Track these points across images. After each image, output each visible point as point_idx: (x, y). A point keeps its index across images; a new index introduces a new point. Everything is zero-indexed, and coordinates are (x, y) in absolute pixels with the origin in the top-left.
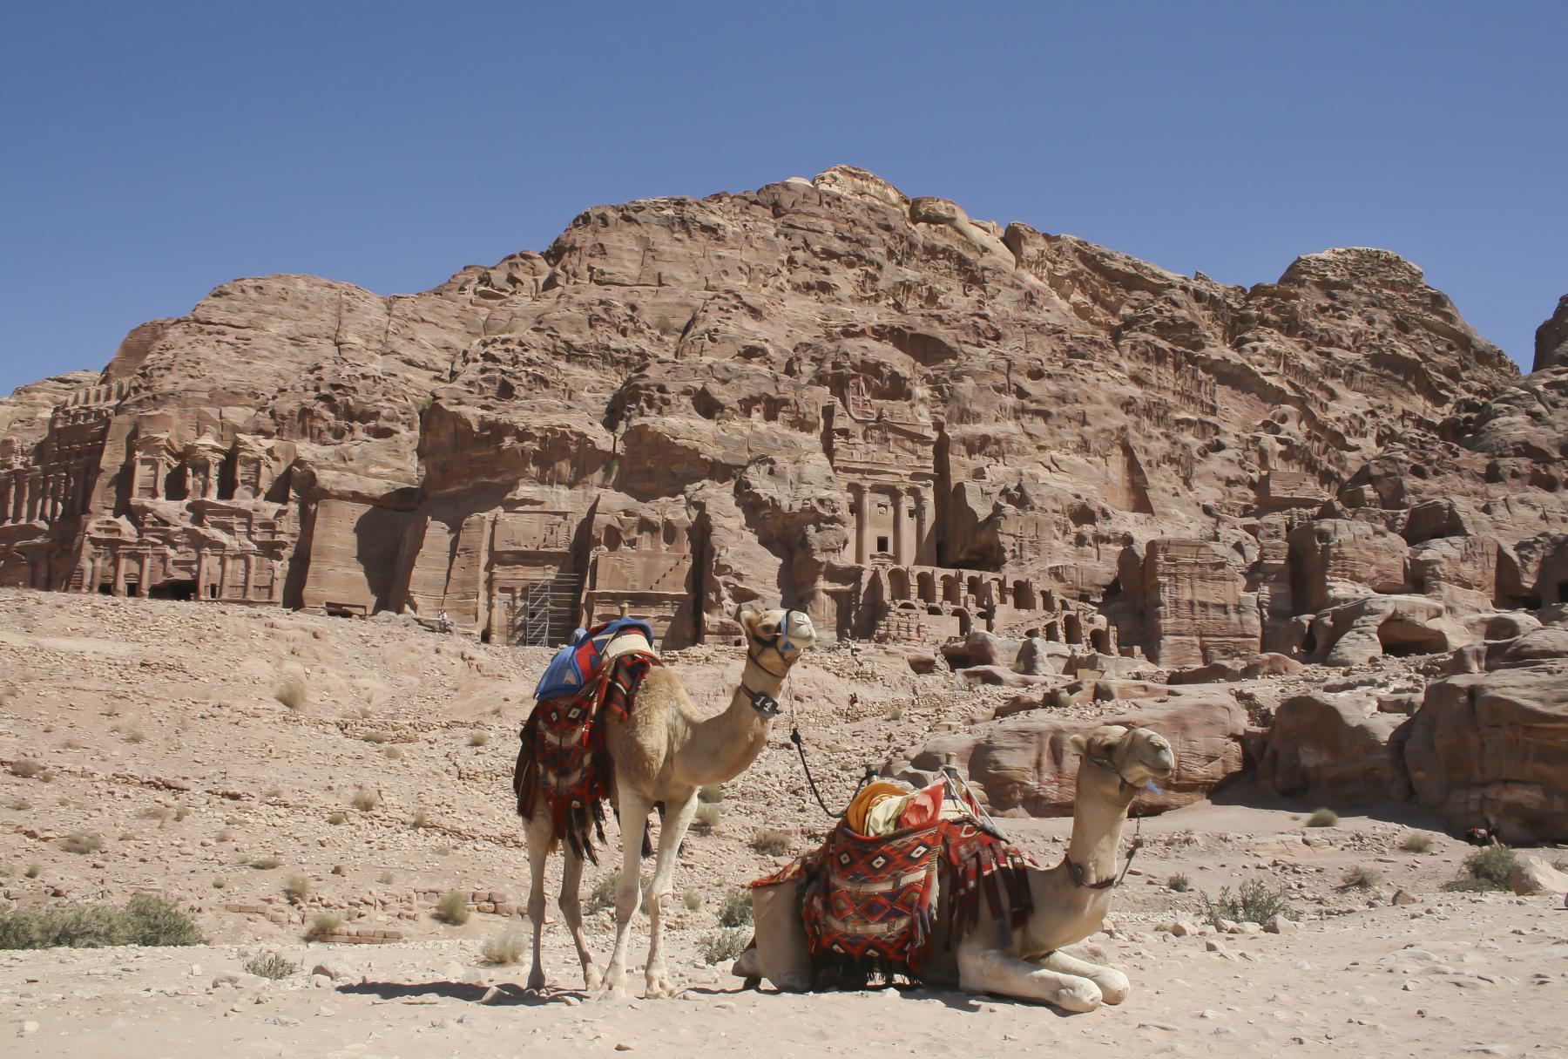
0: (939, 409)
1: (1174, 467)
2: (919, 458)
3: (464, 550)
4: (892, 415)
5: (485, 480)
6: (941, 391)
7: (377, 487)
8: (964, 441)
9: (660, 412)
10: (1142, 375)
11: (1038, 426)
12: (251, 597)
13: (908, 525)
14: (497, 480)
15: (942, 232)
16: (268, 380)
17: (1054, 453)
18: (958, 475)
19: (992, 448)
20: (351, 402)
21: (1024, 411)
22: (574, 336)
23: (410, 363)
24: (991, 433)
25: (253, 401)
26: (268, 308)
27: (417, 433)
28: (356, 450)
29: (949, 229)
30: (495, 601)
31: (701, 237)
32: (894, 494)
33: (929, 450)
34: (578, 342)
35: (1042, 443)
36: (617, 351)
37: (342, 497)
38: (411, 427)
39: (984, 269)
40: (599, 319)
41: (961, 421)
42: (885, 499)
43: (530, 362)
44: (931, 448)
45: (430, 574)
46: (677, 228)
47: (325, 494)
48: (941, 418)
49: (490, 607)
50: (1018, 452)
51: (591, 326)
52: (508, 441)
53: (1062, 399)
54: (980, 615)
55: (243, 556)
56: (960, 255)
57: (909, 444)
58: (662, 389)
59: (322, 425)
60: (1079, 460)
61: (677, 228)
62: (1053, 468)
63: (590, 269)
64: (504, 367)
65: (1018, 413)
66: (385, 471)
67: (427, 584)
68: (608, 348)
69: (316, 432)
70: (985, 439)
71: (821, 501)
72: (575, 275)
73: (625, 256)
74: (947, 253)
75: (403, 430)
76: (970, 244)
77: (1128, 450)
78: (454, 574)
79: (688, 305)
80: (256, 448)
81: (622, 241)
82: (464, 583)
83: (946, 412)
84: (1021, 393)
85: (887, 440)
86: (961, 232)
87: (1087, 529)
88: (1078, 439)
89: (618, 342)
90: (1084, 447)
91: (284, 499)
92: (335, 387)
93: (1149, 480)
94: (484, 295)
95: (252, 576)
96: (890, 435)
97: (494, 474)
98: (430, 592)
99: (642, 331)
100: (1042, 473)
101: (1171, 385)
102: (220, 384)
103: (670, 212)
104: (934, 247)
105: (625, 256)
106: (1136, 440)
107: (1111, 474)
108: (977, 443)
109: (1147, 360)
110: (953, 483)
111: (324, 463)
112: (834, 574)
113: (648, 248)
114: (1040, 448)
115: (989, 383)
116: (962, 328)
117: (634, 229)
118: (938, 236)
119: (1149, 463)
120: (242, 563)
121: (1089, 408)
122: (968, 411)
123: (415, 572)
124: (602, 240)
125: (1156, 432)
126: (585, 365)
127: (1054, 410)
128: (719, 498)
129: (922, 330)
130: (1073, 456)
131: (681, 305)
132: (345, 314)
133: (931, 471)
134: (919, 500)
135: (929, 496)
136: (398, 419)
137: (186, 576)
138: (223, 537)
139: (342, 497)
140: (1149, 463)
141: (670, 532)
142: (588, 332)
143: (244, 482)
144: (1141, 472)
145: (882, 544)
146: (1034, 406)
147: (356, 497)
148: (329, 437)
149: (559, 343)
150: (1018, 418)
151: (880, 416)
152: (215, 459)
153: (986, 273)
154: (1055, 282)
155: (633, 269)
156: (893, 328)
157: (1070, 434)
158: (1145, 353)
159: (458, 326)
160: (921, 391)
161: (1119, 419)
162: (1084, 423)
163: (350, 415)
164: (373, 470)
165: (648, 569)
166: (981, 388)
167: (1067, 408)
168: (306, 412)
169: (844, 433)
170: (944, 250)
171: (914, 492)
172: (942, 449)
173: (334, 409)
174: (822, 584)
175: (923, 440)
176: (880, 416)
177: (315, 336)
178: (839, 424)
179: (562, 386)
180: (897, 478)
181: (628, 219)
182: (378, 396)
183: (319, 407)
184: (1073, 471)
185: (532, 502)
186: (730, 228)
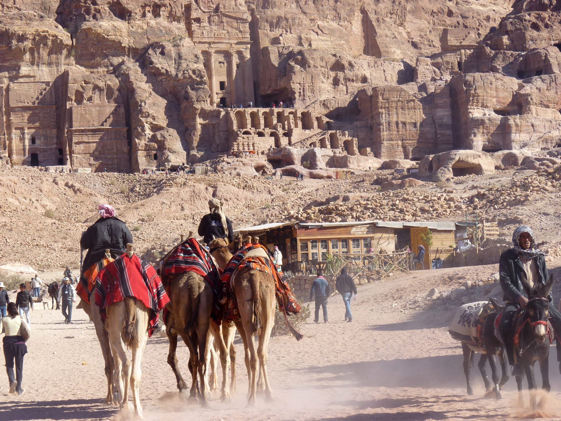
9: (94, 17)
18: (265, 42)
49: (10, 139)
52: (14, 42)
54: (285, 134)
57: (235, 24)
71: (194, 72)
87: (341, 75)
96: (225, 19)
112: (204, 114)
128: (132, 67)
141: (110, 91)
145: (222, 84)
165: (100, 113)
169: (198, 20)
171: (240, 53)
174: (199, 121)
175: (244, 21)
178: (194, 15)
185: (28, 76)
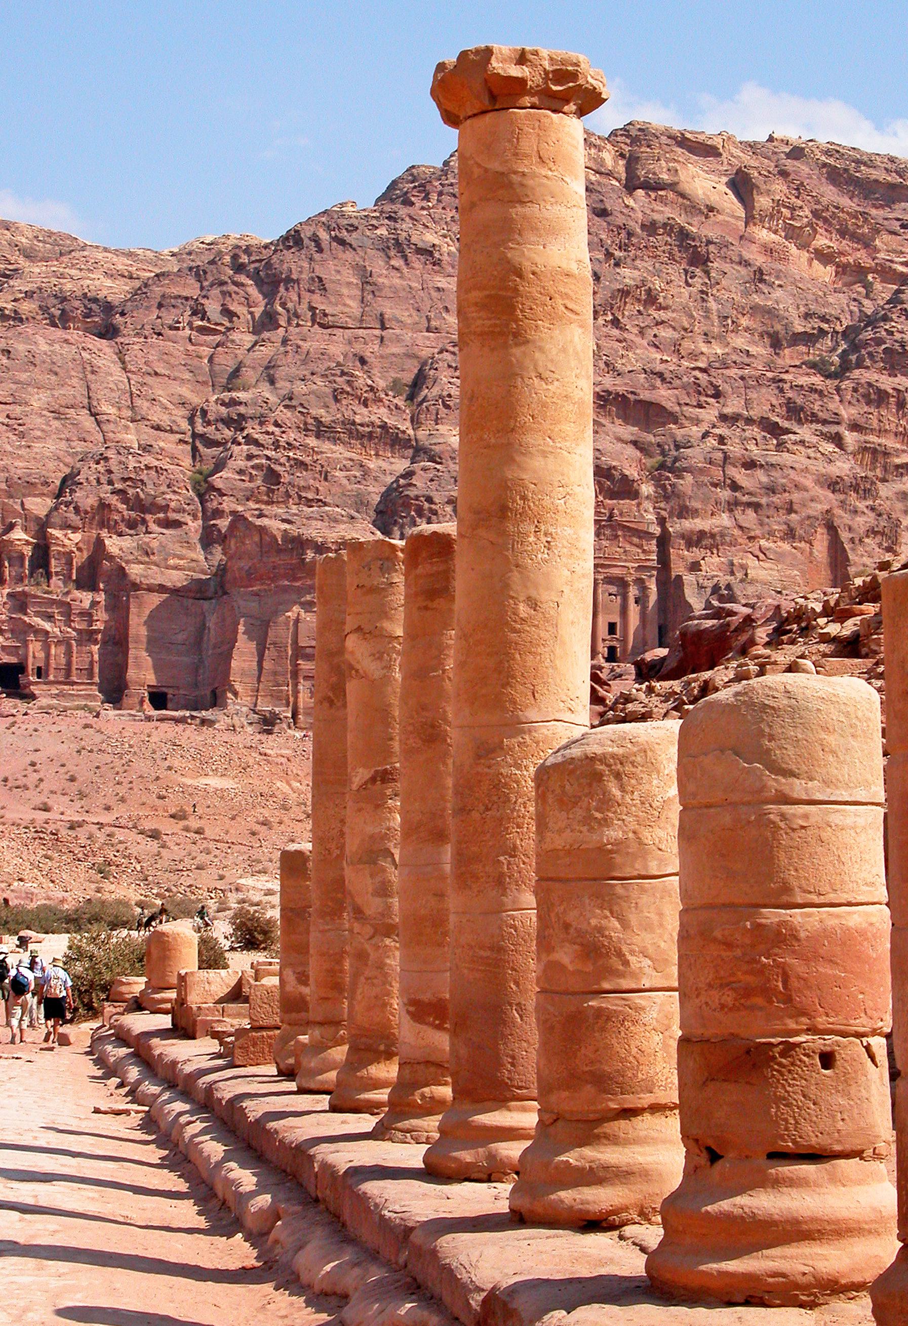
0: (662, 505)
1: (878, 539)
2: (644, 551)
3: (274, 643)
4: (621, 514)
5: (287, 583)
6: (664, 487)
7: (176, 579)
8: (683, 536)
10: (862, 421)
11: (749, 518)
12: (75, 679)
13: (634, 611)
14: (297, 584)
15: (662, 200)
16: (51, 465)
17: (763, 542)
18: (678, 569)
19: (707, 542)
20: (142, 496)
21: (737, 503)
22: (322, 412)
23: (158, 428)
24: (707, 529)
25: (46, 490)
26: (24, 376)
27: (200, 522)
28: (155, 544)
29: (671, 195)
30: (301, 687)
31: (417, 262)
32: (622, 583)
33: (653, 546)
34: (327, 419)
35: (752, 534)
36: (362, 425)
37: (150, 589)
38: (195, 517)
39: (709, 242)
40: (343, 392)
41: (680, 516)
42: (613, 589)
43: (290, 446)
44: (654, 542)
45: (245, 665)
46: (392, 253)
47: (136, 587)
48: (663, 513)
50: (731, 544)
51: (337, 400)
52: (310, 555)
53: (771, 490)
55: (65, 642)
56: (682, 228)
57: (636, 540)
58: (430, 500)
59: (117, 517)
60: (786, 546)
61: (392, 253)
62: (762, 556)
63: (312, 309)
64: (266, 452)
65: (732, 506)
66: (182, 562)
67: (243, 673)
68: (354, 423)
69: (112, 523)
70: (702, 534)
72: (298, 316)
73: (345, 291)
74: (668, 227)
75: (188, 519)
76: (691, 206)
77: (832, 528)
78: (267, 665)
79: (415, 357)
80: (67, 542)
81: (338, 270)
82: (275, 673)
83: (668, 507)
84: (735, 487)
85: (617, 536)
86: (683, 196)
88: (785, 527)
89: (362, 415)
90: (790, 534)
91: (94, 588)
92: (124, 480)
93: (851, 556)
94: (202, 330)
95: (74, 659)
96: (620, 533)
97: (296, 579)
98: (246, 680)
99: (381, 400)
100: (751, 562)
101: (893, 426)
102: (16, 473)
103: (382, 231)
104: (653, 223)
105: (345, 291)
106: (842, 518)
107: (816, 553)
108: (695, 538)
109: (868, 403)
110: (673, 574)
111: (131, 557)
113: (366, 279)
114: (751, 538)
115: (706, 479)
116: (684, 387)
117: (349, 255)
118: (658, 207)
119: (852, 540)
120: (62, 649)
121: (796, 496)
122: (687, 507)
123: (234, 664)
124: (319, 271)
125: (861, 505)
126: (335, 440)
127: (764, 501)
129: (645, 395)
130: (780, 543)
131: (409, 356)
132: (90, 376)
133: (655, 564)
134: (644, 588)
135: (653, 587)
136: (184, 511)
137: (13, 660)
138: (47, 626)
139: (150, 589)
140: (852, 540)
142: (333, 406)
143: (57, 573)
144: (844, 550)
145: (612, 628)
146: (746, 499)
147: (162, 588)
148: (123, 528)
149: (310, 421)
150: (731, 511)
151: (611, 516)
152: (28, 551)
153: (712, 248)
154: (792, 233)
155: (354, 307)
156: (617, 394)
157: (777, 524)
158: (866, 396)
159: (188, 376)
160: (647, 489)
161: (827, 499)
162: (790, 510)
163: (139, 506)
164: (171, 562)
166: (698, 485)
167: (776, 499)
168: (104, 506)
170: (665, 225)
171: (640, 582)
172: (664, 541)
173: (126, 501)
176: (611, 516)
177: (72, 407)
179: (319, 468)
180: (625, 571)
181: (342, 242)
182: (164, 488)
183: (114, 500)
184: (780, 557)
186: (445, 249)
